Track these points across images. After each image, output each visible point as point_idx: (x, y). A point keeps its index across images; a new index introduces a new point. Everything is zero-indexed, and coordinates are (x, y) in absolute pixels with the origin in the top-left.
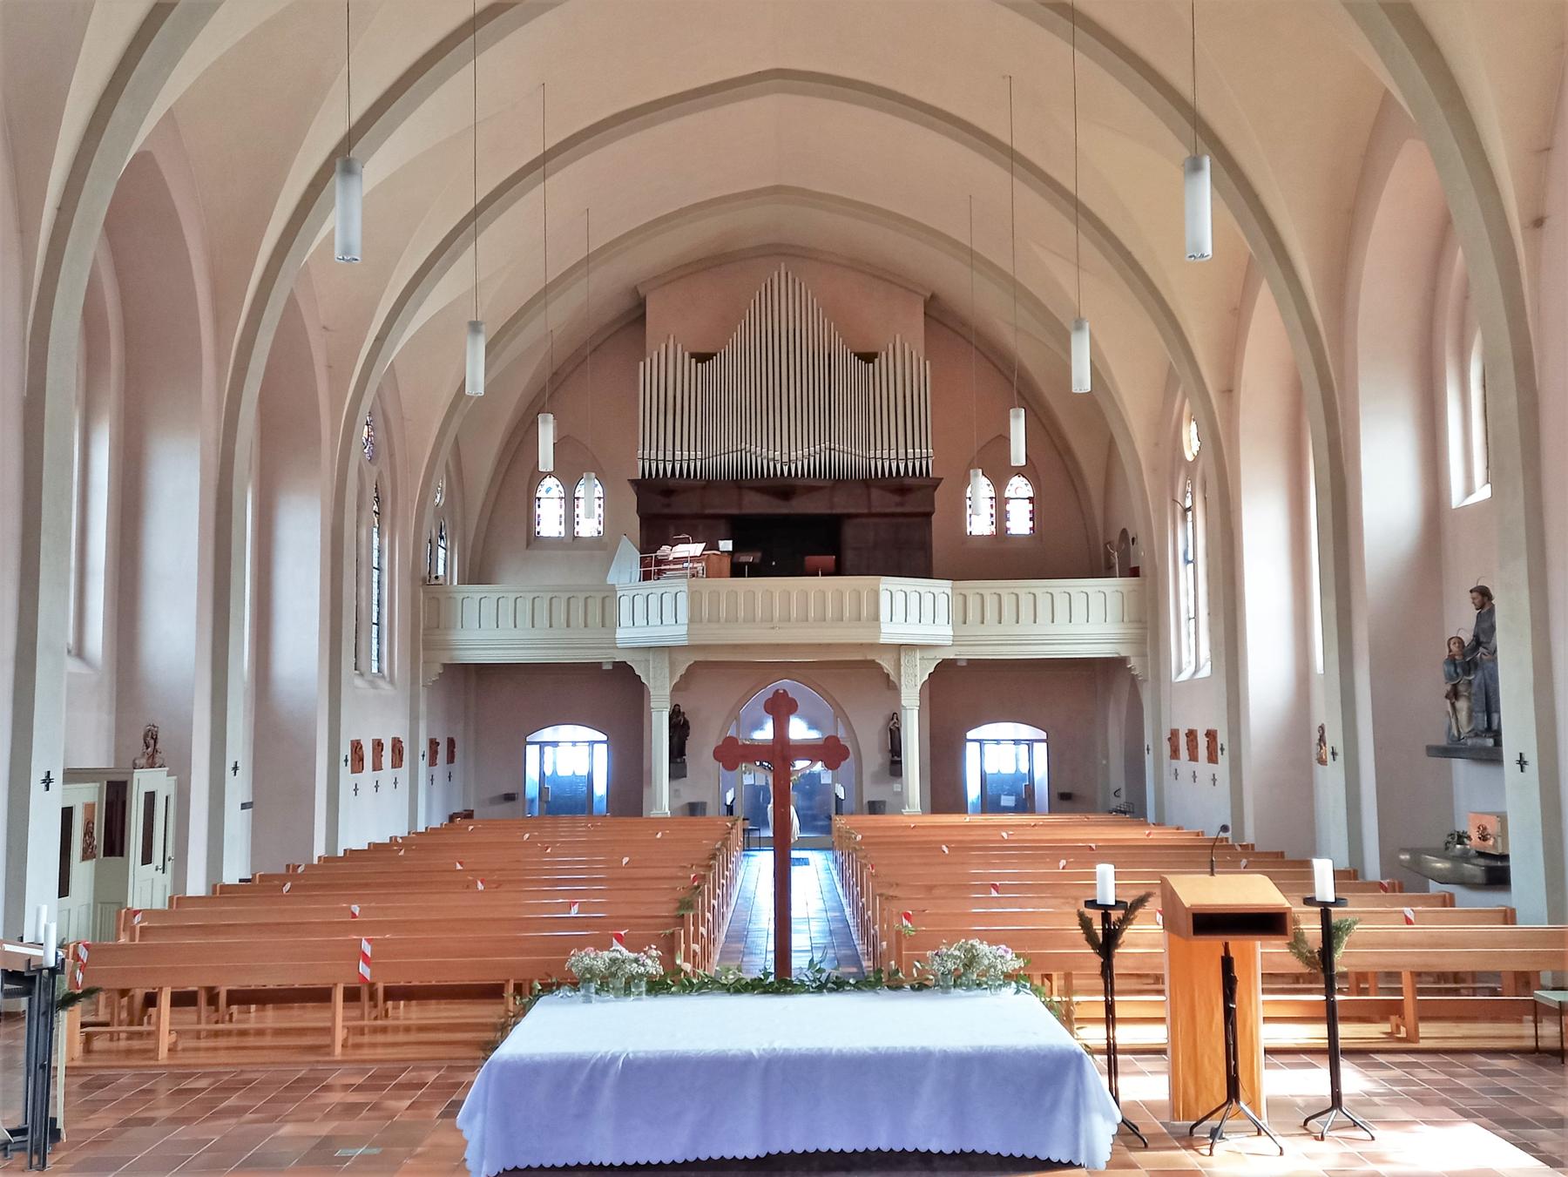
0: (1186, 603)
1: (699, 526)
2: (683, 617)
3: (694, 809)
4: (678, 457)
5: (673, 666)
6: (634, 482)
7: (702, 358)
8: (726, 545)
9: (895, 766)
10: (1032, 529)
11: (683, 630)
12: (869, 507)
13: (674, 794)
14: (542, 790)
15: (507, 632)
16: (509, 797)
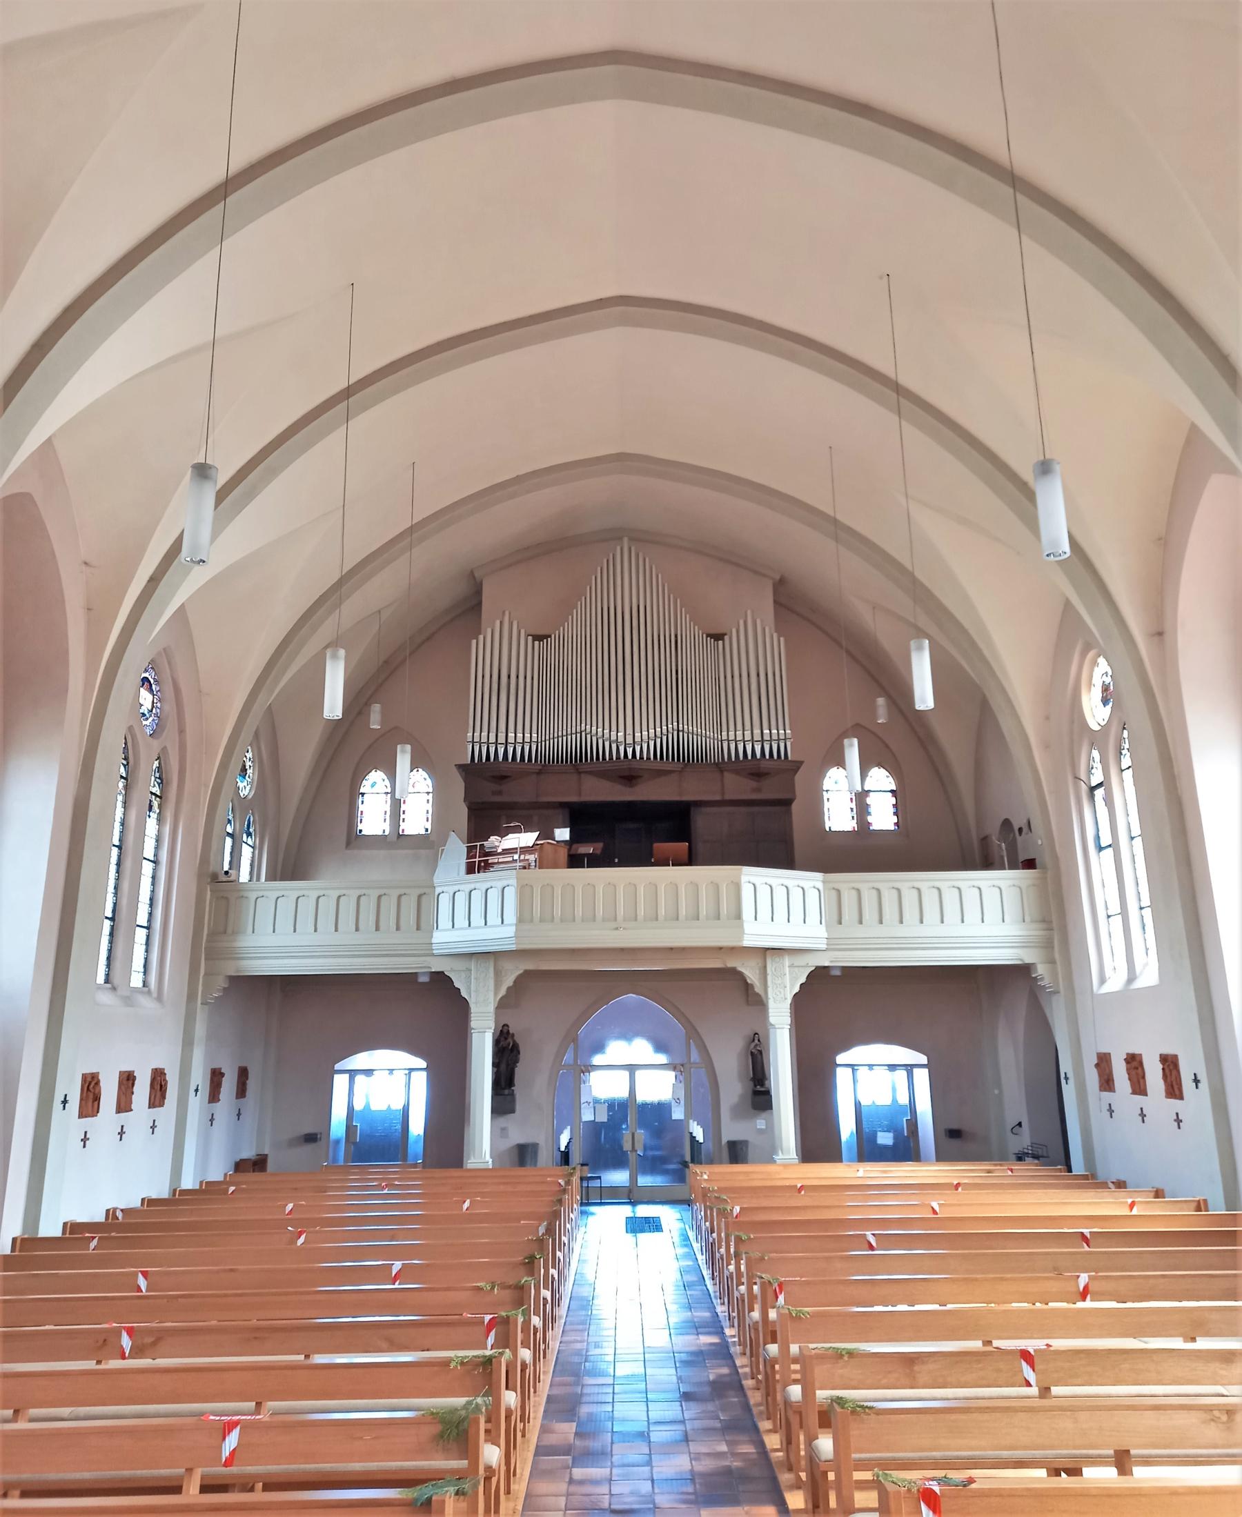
0: (1107, 895)
1: (530, 814)
2: (511, 916)
3: (524, 1154)
4: (511, 740)
5: (498, 974)
6: (462, 768)
7: (539, 638)
8: (563, 834)
9: (760, 1098)
10: (897, 824)
11: (509, 931)
12: (723, 794)
13: (499, 1133)
14: (350, 1128)
15: (305, 937)
16: (311, 1138)
